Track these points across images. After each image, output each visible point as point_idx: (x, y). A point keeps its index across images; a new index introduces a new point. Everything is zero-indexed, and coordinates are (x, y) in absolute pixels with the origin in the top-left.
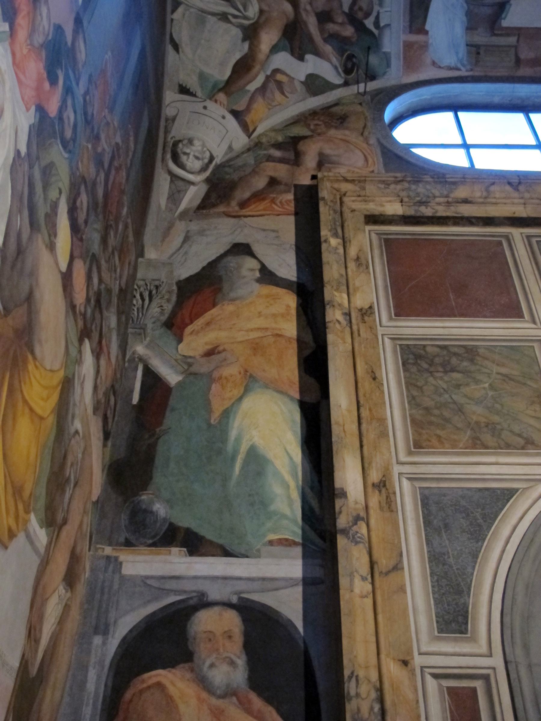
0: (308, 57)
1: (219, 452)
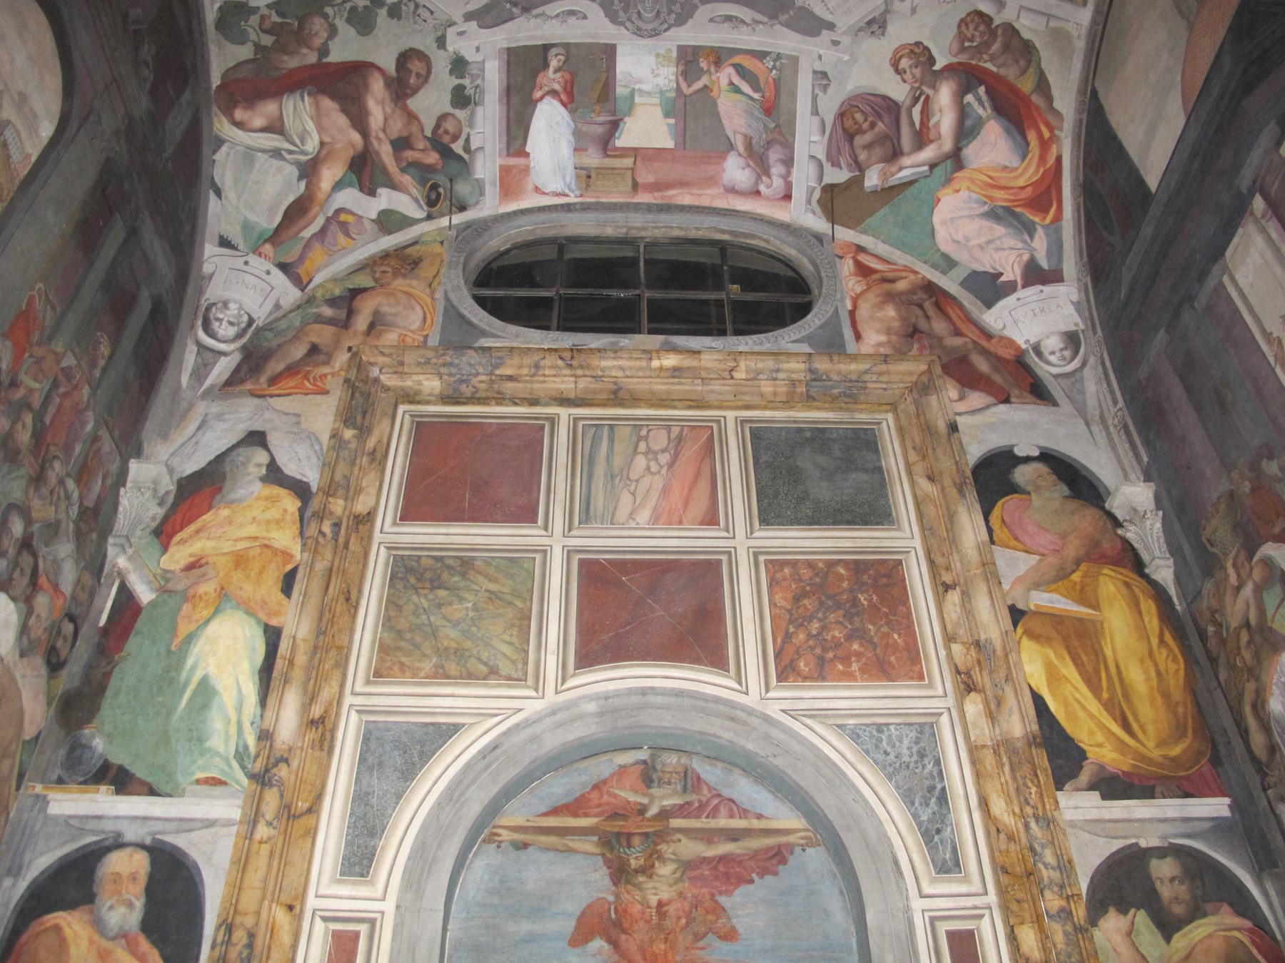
0: (381, 191)
1: (172, 682)
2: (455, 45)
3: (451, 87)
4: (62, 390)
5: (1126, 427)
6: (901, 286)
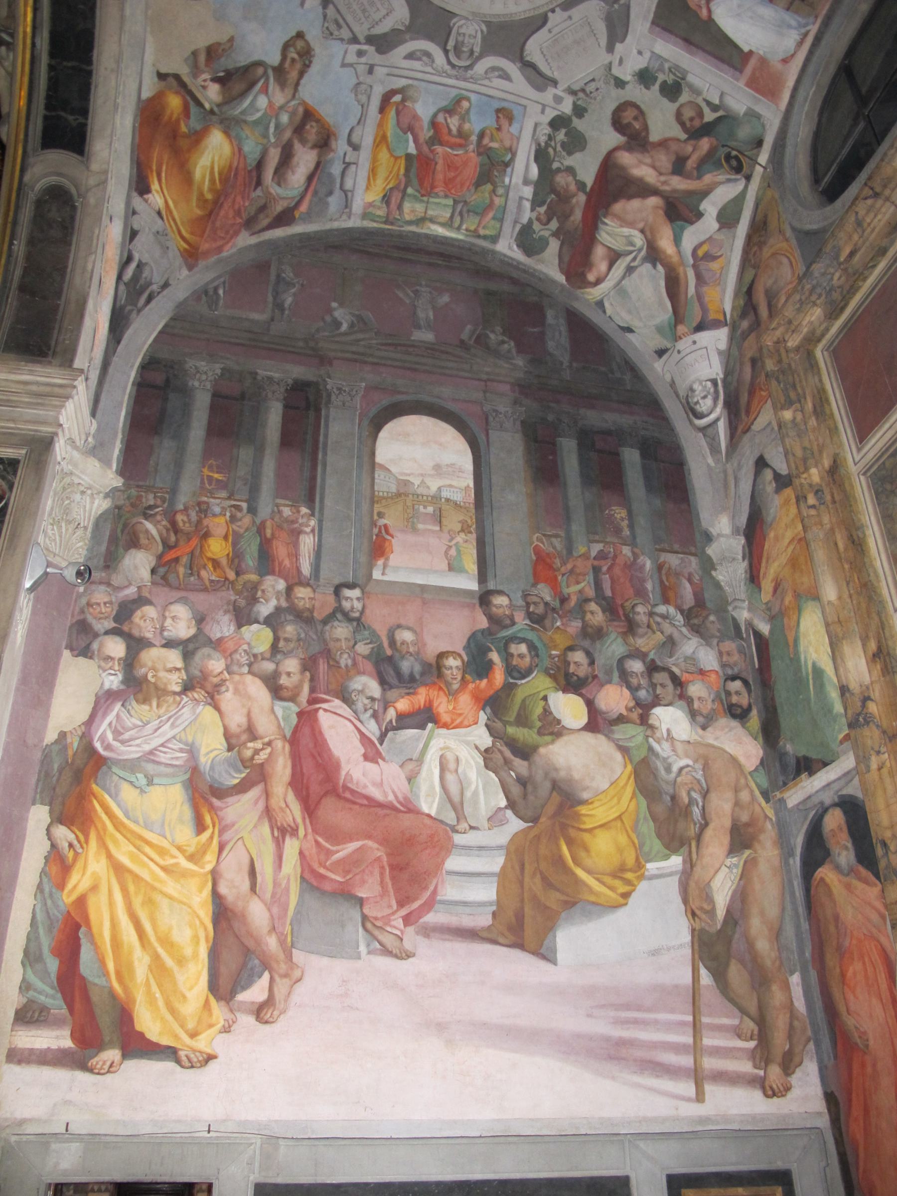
2: (626, 73)
3: (658, 93)
4: (605, 569)
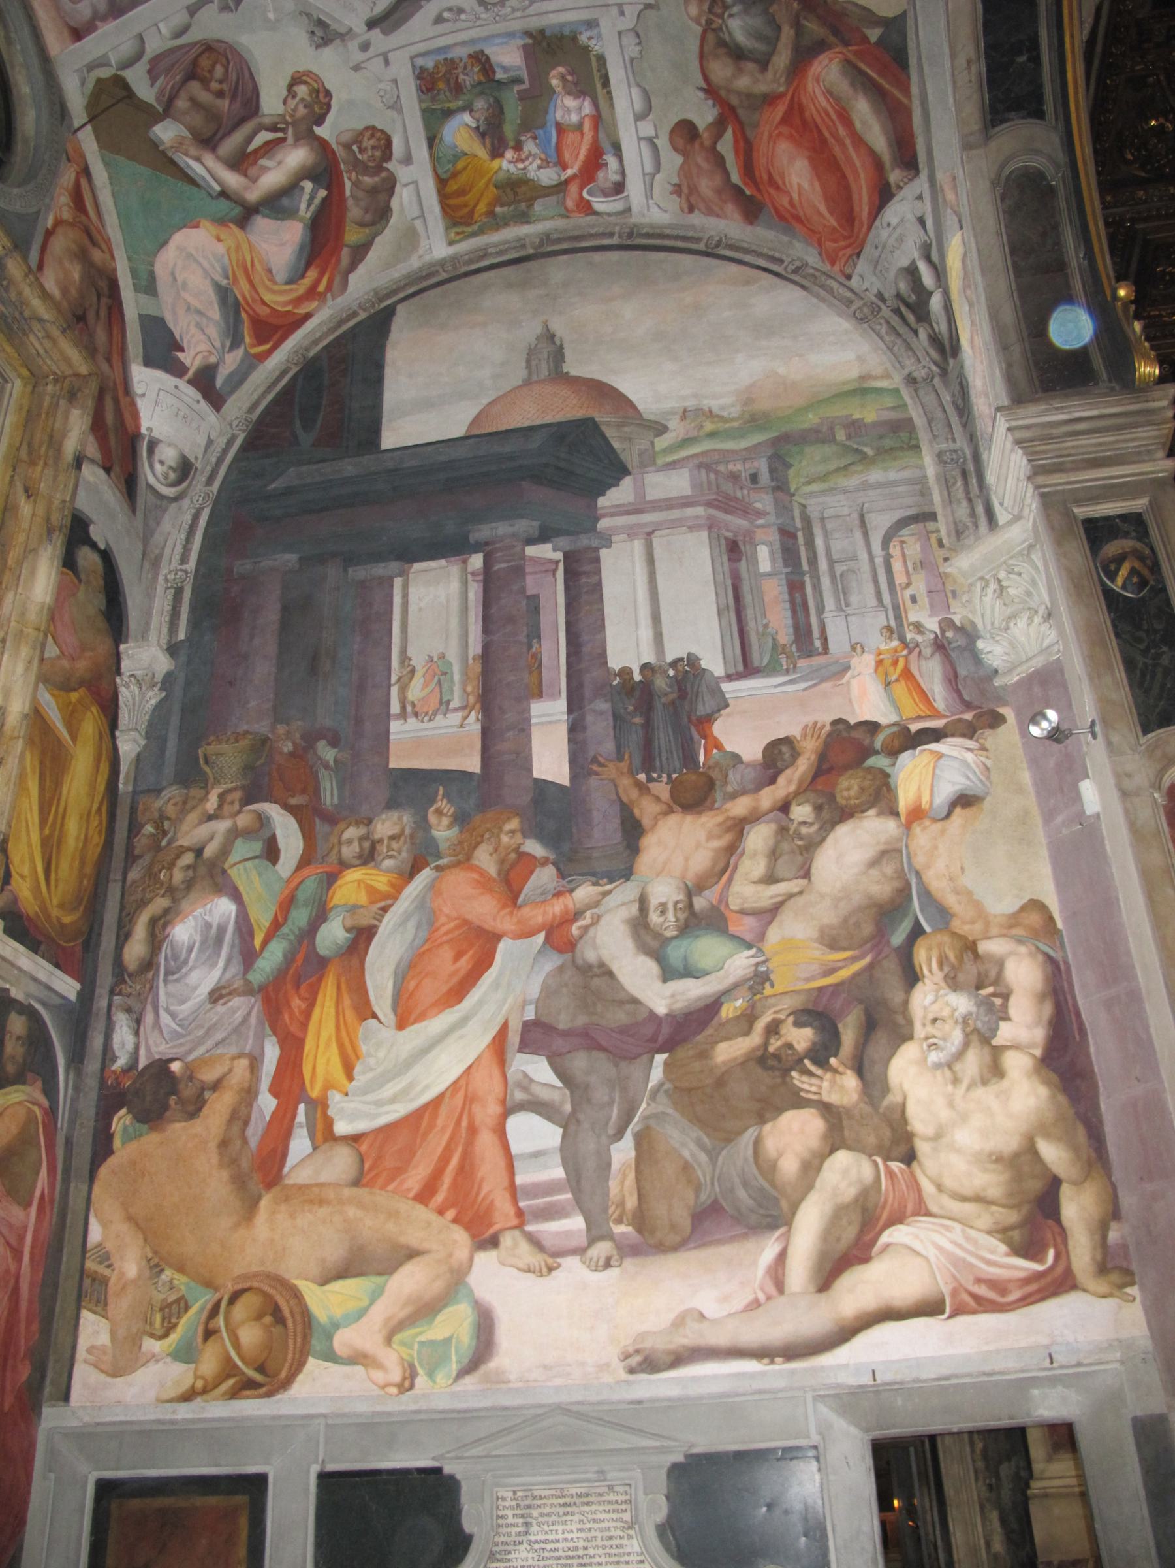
5: (179, 592)
6: (97, 255)
